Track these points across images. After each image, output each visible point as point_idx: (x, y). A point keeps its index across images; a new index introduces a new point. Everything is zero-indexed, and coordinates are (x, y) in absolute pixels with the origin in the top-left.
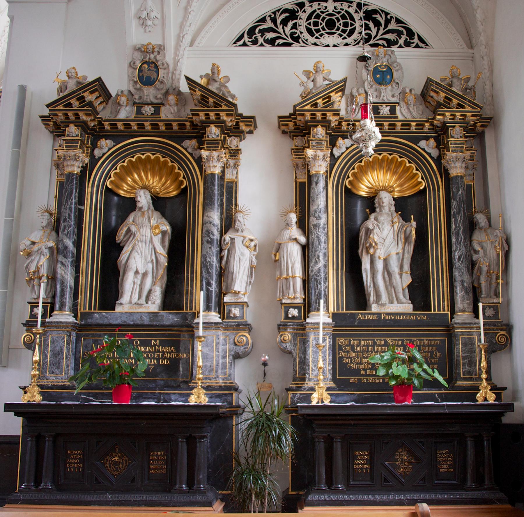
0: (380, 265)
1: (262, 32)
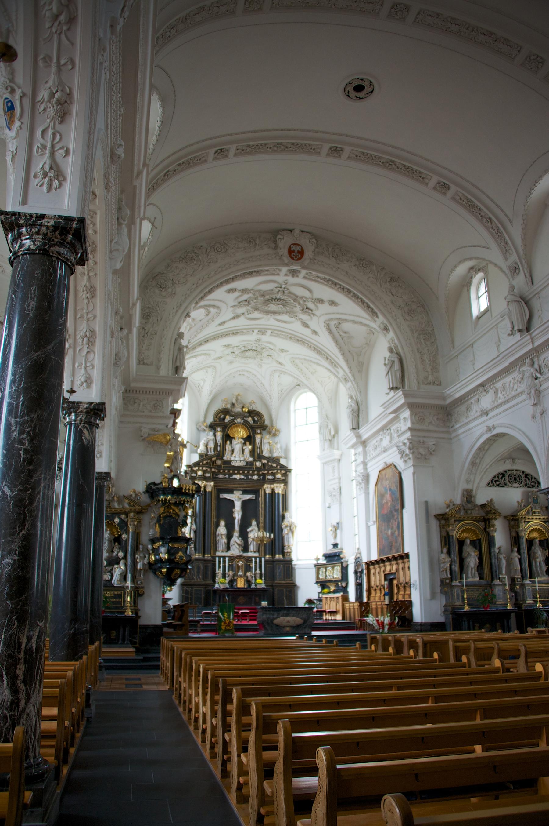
0: (538, 564)
1: (495, 481)
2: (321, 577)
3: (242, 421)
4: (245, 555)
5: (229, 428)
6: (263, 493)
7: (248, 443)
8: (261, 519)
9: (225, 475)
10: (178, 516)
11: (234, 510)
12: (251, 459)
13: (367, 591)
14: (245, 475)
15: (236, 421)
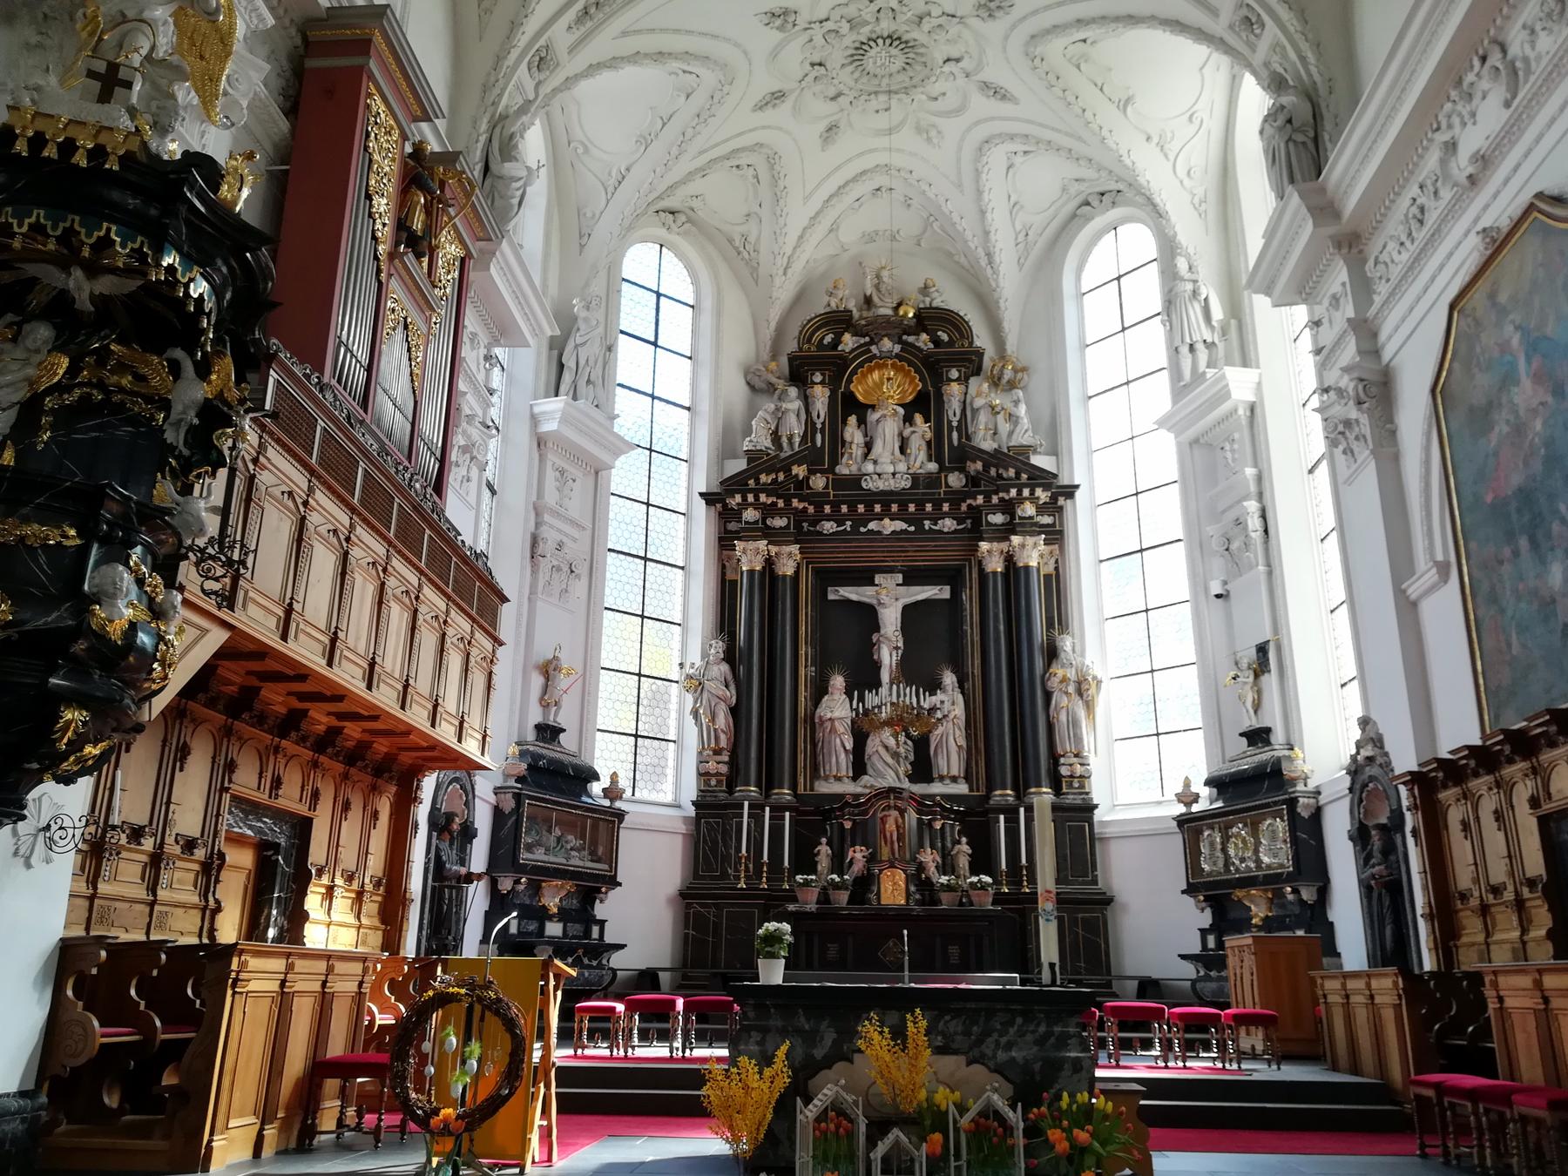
2: (1206, 867)
3: (897, 348)
4: (919, 789)
5: (854, 372)
6: (975, 575)
7: (918, 418)
8: (974, 665)
9: (840, 523)
10: (166, 405)
11: (875, 638)
12: (933, 467)
13: (1429, 917)
14: (908, 522)
15: (873, 348)
